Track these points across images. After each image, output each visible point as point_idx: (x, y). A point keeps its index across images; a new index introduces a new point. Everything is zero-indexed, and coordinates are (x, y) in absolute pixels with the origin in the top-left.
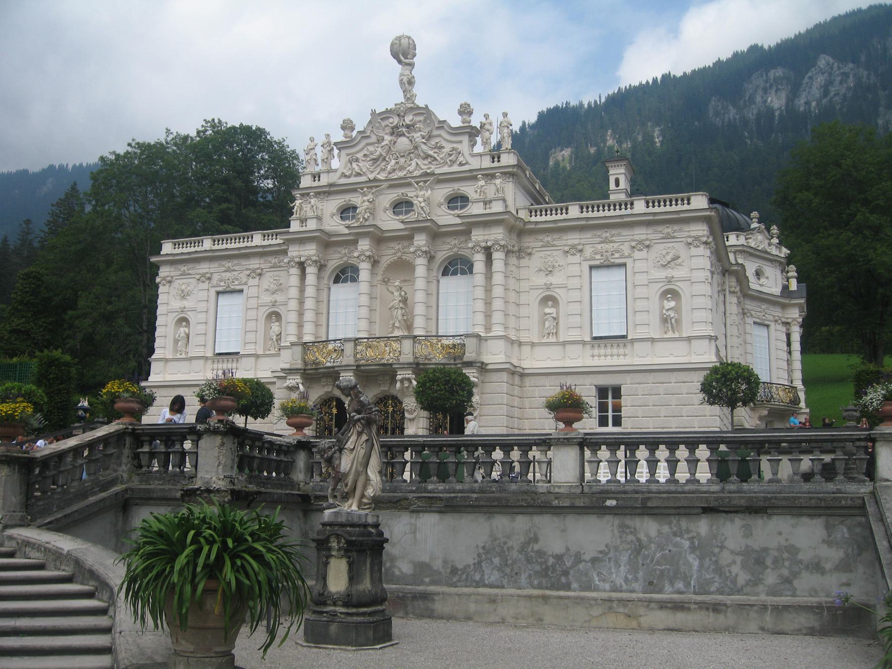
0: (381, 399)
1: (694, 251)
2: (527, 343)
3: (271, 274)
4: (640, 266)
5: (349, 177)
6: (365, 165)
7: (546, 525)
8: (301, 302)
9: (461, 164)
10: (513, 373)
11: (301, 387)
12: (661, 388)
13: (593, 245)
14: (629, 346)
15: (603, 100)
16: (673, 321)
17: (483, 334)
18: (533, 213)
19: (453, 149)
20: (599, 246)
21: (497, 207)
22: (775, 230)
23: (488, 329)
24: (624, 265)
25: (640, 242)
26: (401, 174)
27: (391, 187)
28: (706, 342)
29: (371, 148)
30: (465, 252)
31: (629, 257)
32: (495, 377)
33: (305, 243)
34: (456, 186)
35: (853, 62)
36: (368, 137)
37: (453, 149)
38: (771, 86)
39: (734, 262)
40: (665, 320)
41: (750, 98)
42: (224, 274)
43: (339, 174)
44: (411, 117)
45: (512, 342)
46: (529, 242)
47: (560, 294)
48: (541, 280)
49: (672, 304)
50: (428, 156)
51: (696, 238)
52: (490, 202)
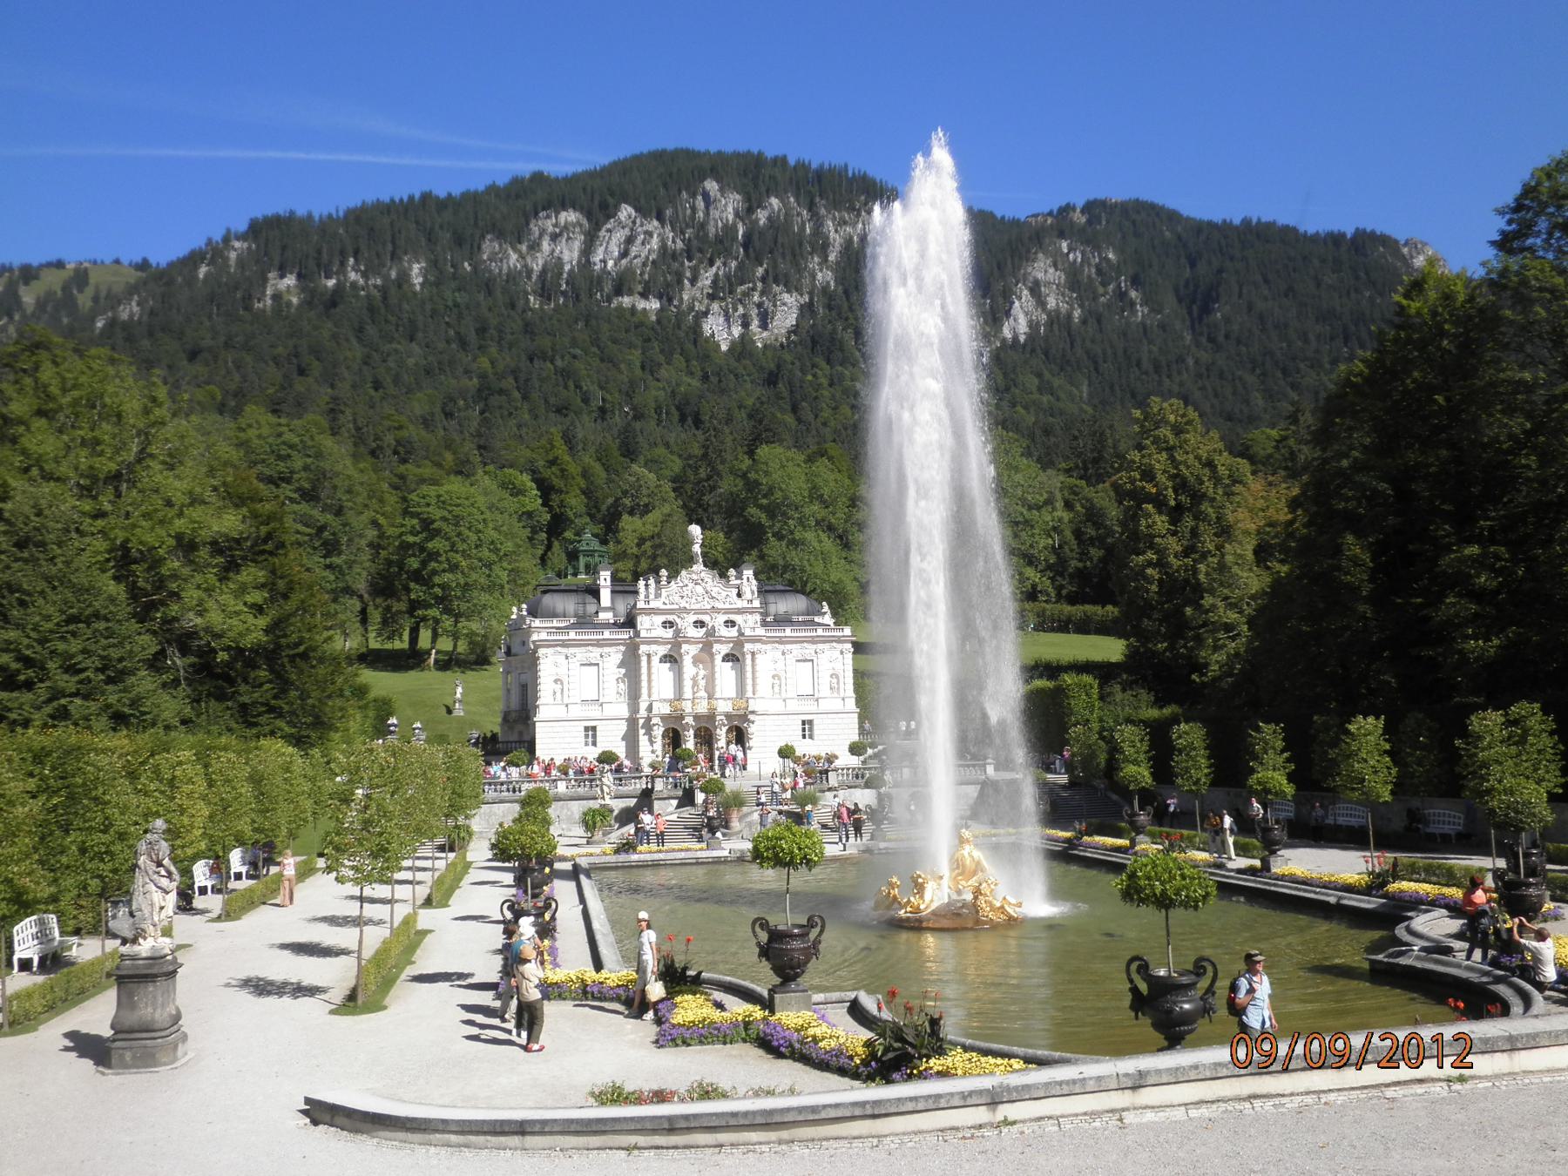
6: (677, 598)
15: (341, 214)
38: (560, 234)
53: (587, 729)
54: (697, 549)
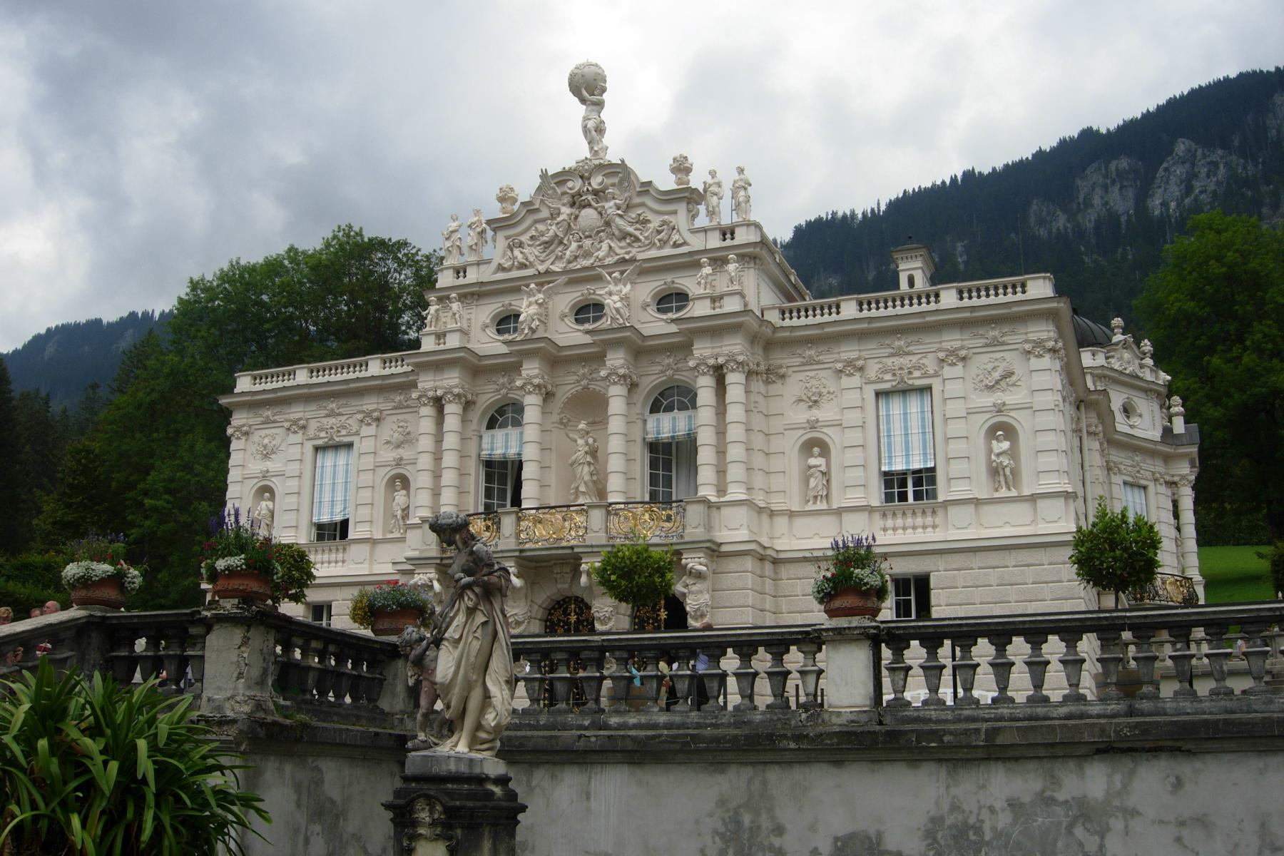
0: (558, 603)
1: (1035, 363)
2: (781, 513)
3: (394, 418)
4: (953, 388)
5: (509, 270)
6: (532, 252)
8: (438, 458)
9: (676, 245)
10: (762, 559)
11: (437, 586)
12: (993, 576)
13: (880, 362)
14: (940, 512)
15: (883, 208)
16: (1008, 471)
17: (713, 499)
18: (787, 315)
19: (664, 223)
20: (889, 361)
21: (731, 305)
22: (1147, 345)
23: (721, 491)
24: (929, 389)
25: (952, 352)
27: (571, 282)
28: (1060, 502)
29: (541, 227)
30: (683, 377)
31: (936, 375)
32: (733, 564)
33: (443, 369)
34: (669, 278)
35: (1223, 147)
36: (537, 210)
37: (664, 223)
39: (1092, 388)
40: (995, 472)
41: (1085, 199)
42: (325, 421)
43: (494, 265)
44: (599, 179)
45: (760, 510)
46: (783, 359)
47: (833, 437)
48: (802, 415)
49: (1006, 445)
50: (624, 236)
51: (1039, 343)
52: (721, 297)
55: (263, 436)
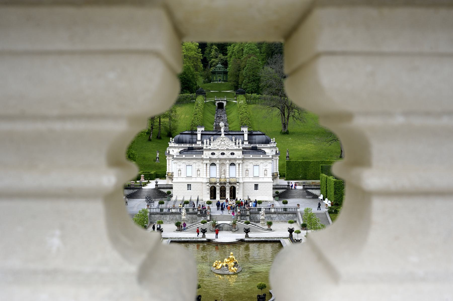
4: (262, 166)
6: (216, 146)
7: (271, 215)
23: (239, 176)
26: (223, 148)
46: (244, 161)
48: (246, 167)
53: (188, 185)
54: (222, 130)
55: (179, 163)
